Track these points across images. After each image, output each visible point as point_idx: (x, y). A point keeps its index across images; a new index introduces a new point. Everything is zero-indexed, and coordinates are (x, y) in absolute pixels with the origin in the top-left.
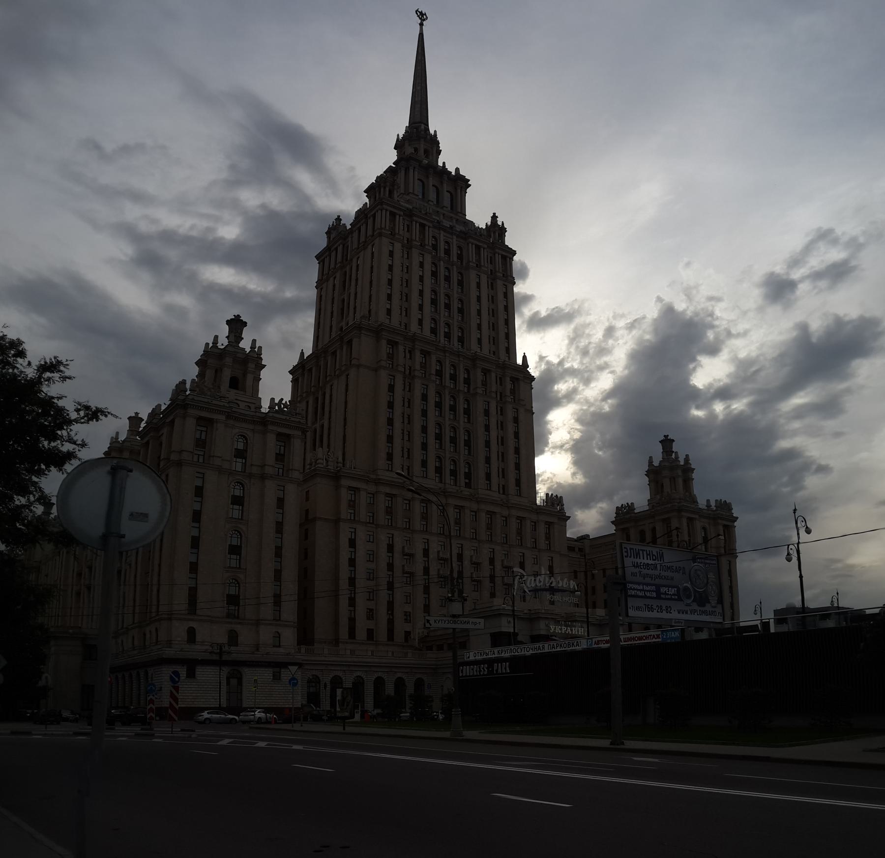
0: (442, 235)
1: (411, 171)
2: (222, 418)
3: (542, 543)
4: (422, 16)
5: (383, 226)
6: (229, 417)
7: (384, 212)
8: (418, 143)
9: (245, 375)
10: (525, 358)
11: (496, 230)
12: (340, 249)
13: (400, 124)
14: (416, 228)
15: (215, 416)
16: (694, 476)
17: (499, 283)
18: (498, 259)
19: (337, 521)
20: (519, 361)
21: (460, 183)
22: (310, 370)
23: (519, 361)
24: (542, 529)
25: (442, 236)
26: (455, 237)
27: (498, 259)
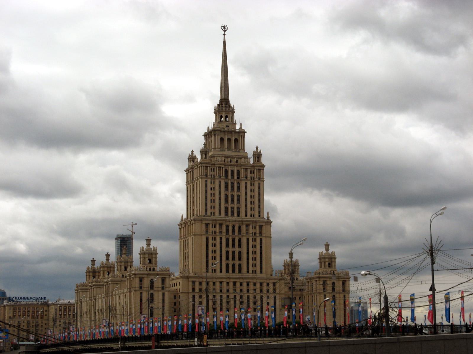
0: (229, 168)
1: (217, 136)
2: (146, 276)
3: (271, 290)
5: (202, 174)
6: (148, 275)
7: (202, 167)
9: (152, 258)
10: (268, 213)
11: (258, 155)
12: (191, 172)
14: (217, 170)
15: (143, 276)
17: (256, 184)
18: (256, 172)
19: (188, 293)
20: (265, 217)
21: (242, 133)
22: (183, 227)
23: (265, 217)
24: (271, 285)
25: (229, 169)
26: (235, 167)
27: (256, 172)
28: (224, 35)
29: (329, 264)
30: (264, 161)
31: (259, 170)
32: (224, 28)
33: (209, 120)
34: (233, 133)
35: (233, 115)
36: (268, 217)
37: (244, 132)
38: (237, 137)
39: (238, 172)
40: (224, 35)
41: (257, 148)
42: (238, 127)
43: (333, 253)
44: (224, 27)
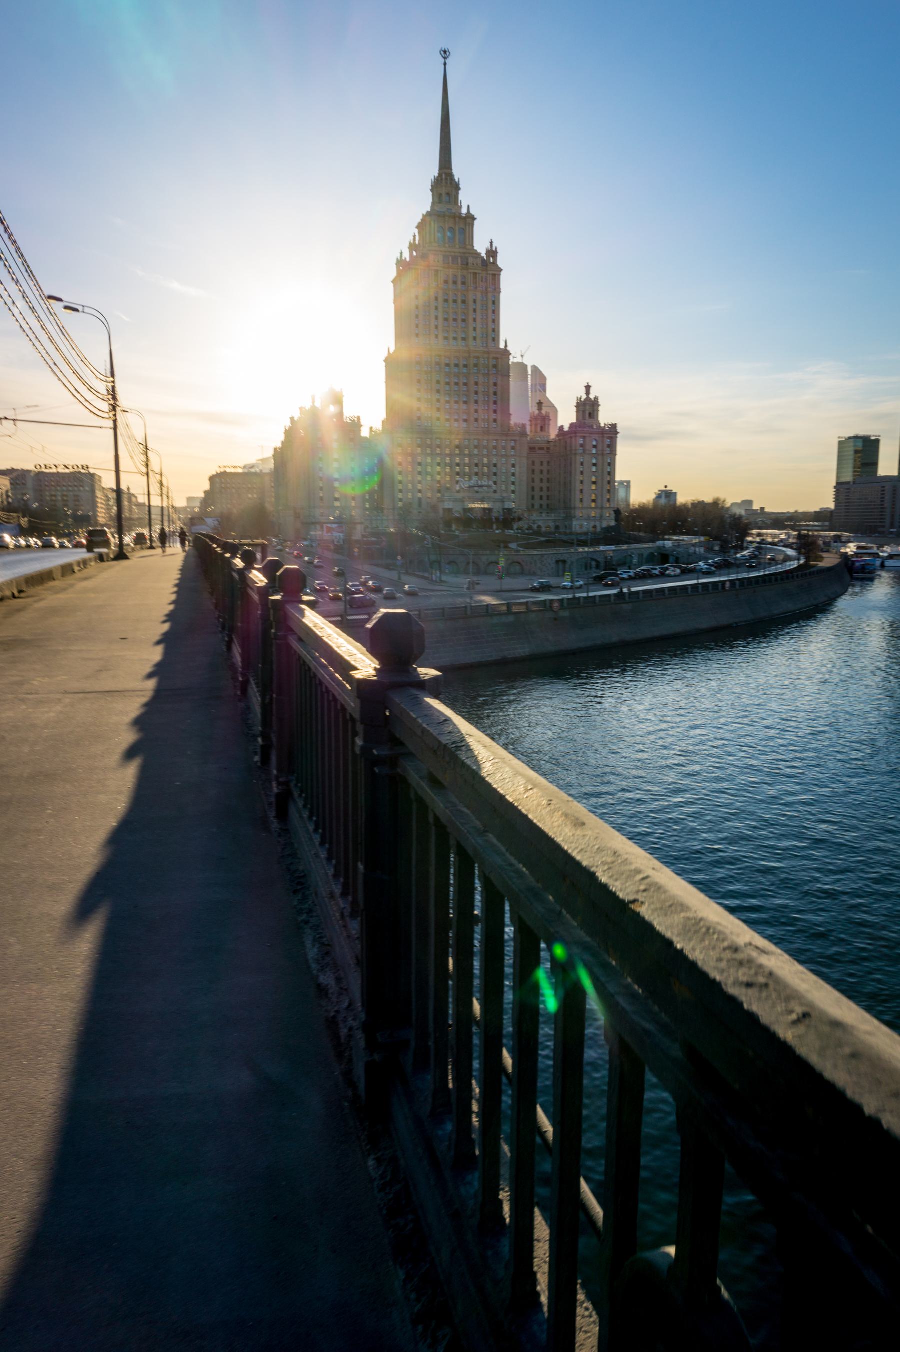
4: (445, 54)
8: (446, 186)
11: (492, 253)
13: (434, 171)
16: (600, 408)
17: (490, 295)
20: (502, 346)
27: (490, 278)
28: (445, 64)
29: (590, 414)
30: (500, 263)
31: (494, 275)
32: (445, 54)
33: (424, 202)
34: (457, 219)
35: (458, 194)
36: (506, 346)
37: (474, 219)
38: (462, 226)
39: (464, 277)
40: (445, 64)
41: (491, 243)
42: (464, 211)
43: (596, 399)
44: (445, 52)
